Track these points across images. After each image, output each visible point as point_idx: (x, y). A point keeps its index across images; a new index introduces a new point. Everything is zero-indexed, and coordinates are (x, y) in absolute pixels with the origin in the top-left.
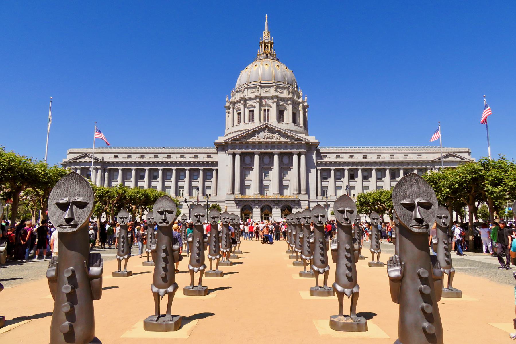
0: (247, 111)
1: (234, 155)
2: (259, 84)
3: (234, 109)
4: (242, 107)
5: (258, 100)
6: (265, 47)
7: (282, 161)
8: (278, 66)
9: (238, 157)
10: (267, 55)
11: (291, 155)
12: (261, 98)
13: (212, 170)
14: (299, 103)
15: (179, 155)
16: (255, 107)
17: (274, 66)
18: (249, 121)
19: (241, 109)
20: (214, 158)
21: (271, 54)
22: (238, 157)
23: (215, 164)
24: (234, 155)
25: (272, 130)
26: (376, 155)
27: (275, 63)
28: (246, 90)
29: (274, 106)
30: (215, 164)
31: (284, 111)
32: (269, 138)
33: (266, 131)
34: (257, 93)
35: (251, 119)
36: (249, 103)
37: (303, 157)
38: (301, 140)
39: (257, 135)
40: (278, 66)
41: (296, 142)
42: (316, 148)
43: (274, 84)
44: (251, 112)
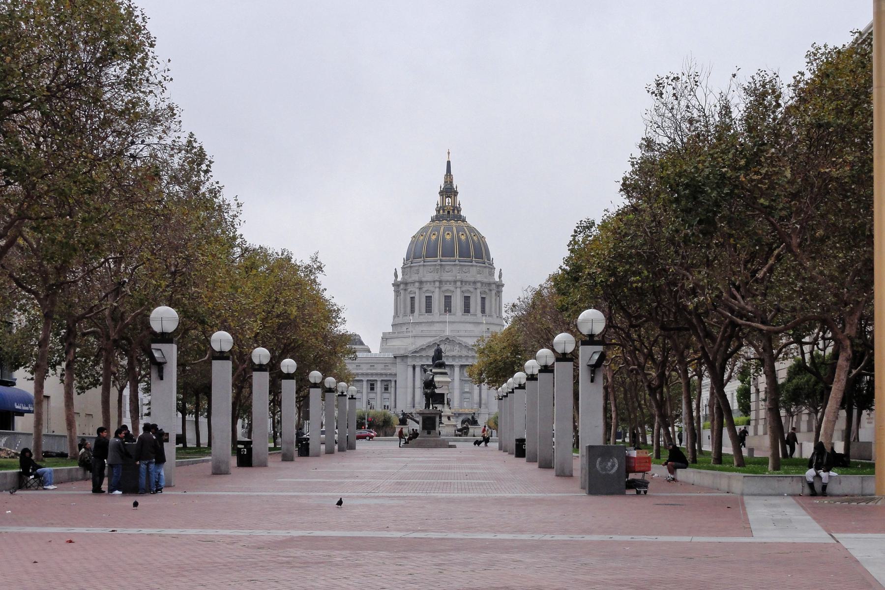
1: (414, 367)
2: (439, 262)
3: (405, 290)
4: (417, 291)
5: (437, 284)
9: (418, 370)
10: (449, 212)
14: (489, 284)
20: (393, 371)
22: (418, 370)
24: (414, 367)
35: (429, 309)
36: (426, 287)
43: (457, 262)
44: (429, 299)
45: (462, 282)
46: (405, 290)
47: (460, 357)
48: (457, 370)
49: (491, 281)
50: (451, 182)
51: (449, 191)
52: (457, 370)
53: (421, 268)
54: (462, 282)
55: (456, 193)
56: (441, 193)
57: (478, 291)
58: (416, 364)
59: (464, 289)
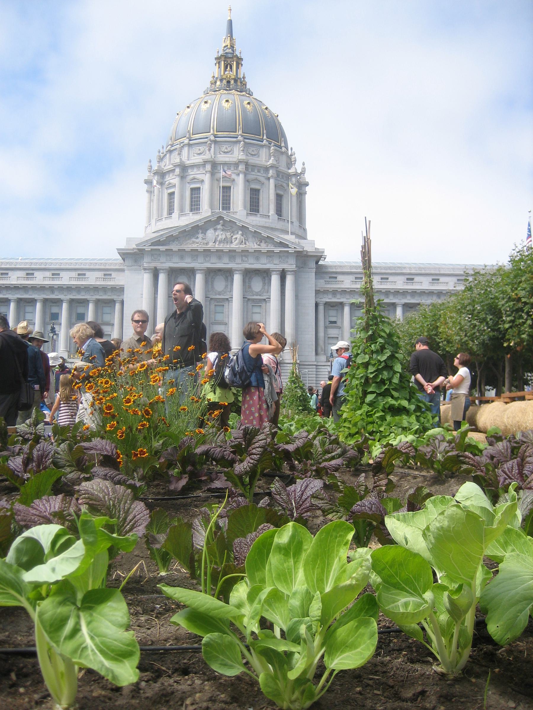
0: (188, 187)
2: (212, 138)
4: (176, 181)
5: (208, 167)
6: (226, 68)
7: (250, 287)
8: (249, 103)
9: (162, 278)
10: (228, 82)
11: (265, 274)
12: (215, 165)
13: (112, 302)
14: (288, 177)
15: (48, 274)
16: (202, 181)
17: (242, 102)
18: (191, 210)
19: (175, 186)
20: (118, 280)
21: (236, 81)
22: (162, 278)
23: (121, 290)
25: (230, 226)
26: (430, 279)
27: (243, 98)
28: (186, 149)
29: (240, 180)
30: (121, 290)
31: (258, 191)
32: (225, 241)
33: (219, 227)
34: (207, 156)
37: (289, 280)
38: (287, 246)
39: (200, 236)
40: (249, 103)
41: (277, 250)
42: (317, 262)
43: (240, 138)
44: (195, 191)
45: (247, 164)
46: (162, 184)
47: (245, 253)
48: (237, 278)
49: (292, 171)
50: (232, 47)
51: (229, 59)
52: (237, 278)
53: (186, 149)
54: (247, 164)
55: (239, 61)
56: (218, 59)
57: (272, 181)
58: (159, 265)
59: (250, 177)
